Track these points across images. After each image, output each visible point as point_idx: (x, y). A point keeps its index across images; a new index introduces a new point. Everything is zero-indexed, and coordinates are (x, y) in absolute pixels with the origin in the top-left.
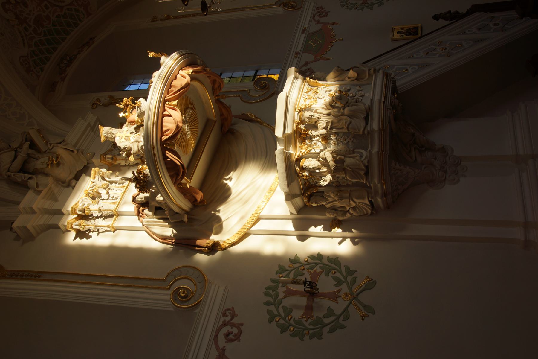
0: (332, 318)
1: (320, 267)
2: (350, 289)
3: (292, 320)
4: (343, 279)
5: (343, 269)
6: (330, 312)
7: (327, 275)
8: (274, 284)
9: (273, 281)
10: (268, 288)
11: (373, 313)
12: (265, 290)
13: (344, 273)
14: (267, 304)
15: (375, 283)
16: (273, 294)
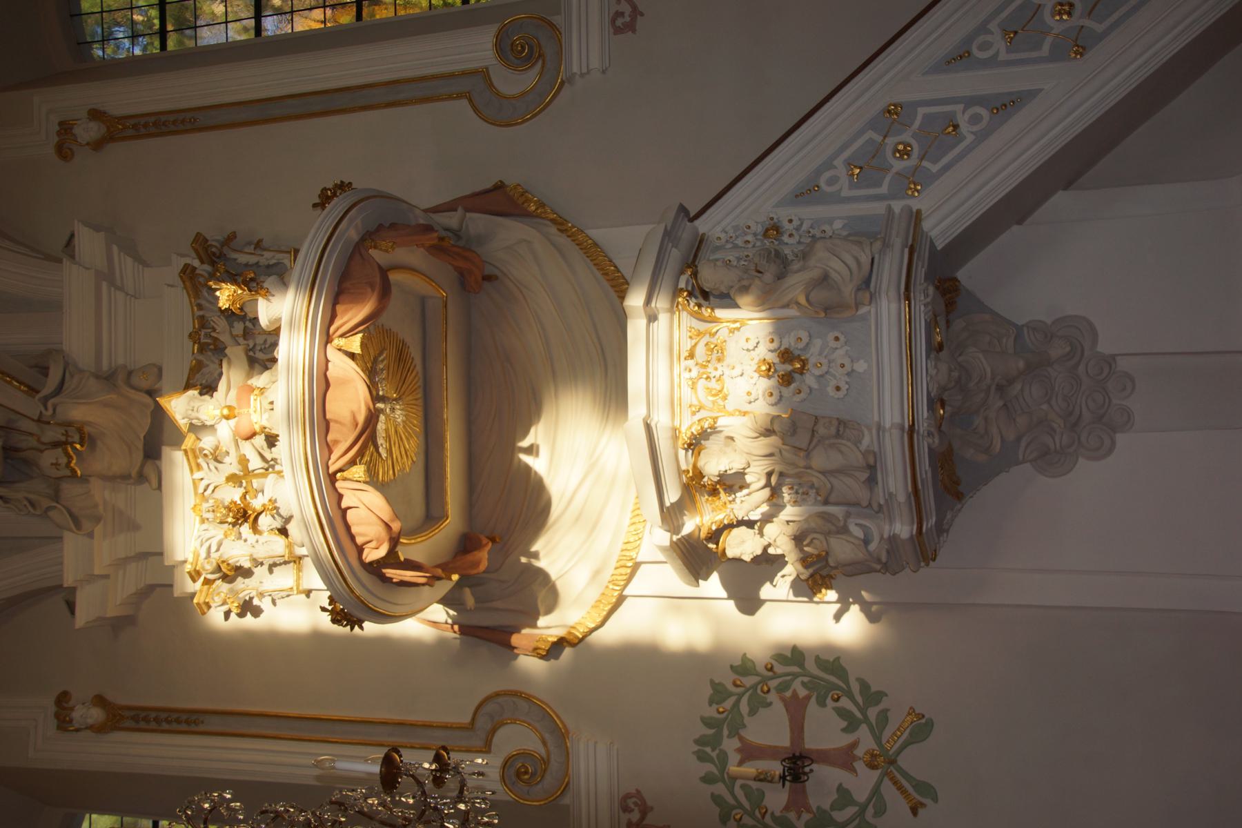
0: (850, 811)
1: (803, 684)
2: (878, 740)
3: (768, 819)
4: (858, 715)
5: (855, 688)
6: (844, 796)
7: (822, 704)
8: (711, 732)
9: (707, 722)
10: (700, 741)
11: (935, 800)
12: (696, 748)
13: (859, 699)
14: (708, 779)
15: (930, 724)
16: (714, 755)
